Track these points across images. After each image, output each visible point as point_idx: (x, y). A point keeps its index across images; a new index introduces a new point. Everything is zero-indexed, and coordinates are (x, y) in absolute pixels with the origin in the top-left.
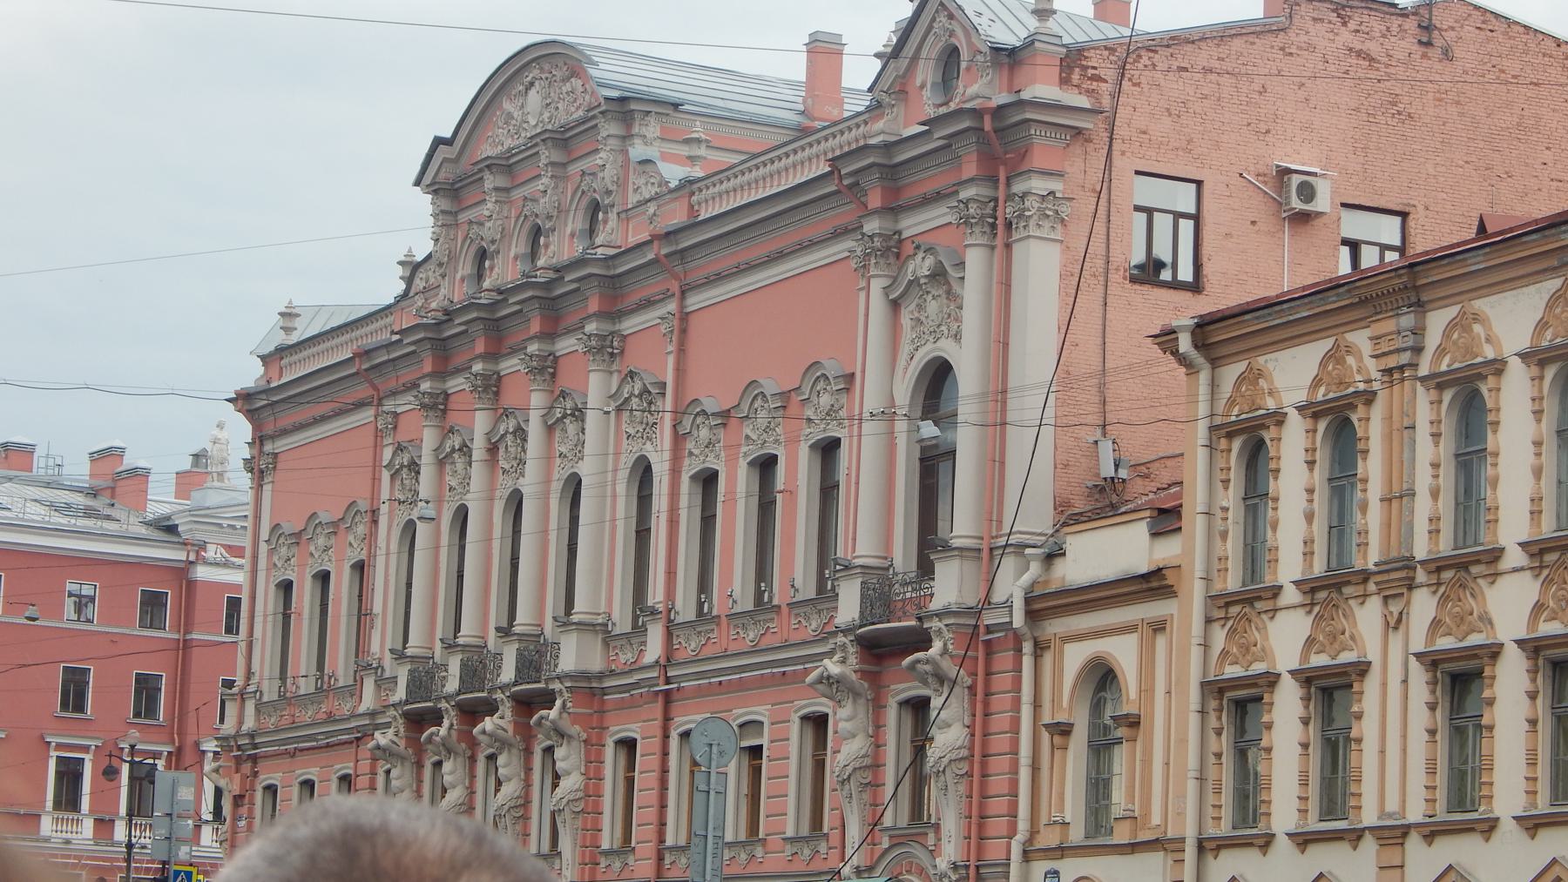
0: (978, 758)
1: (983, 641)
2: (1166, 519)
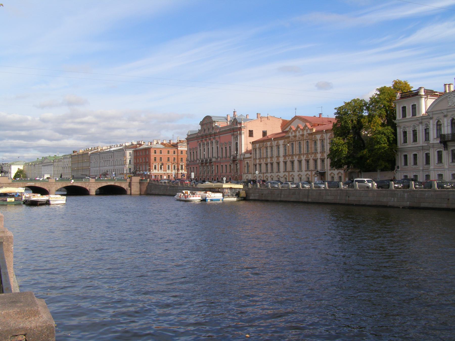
0: (241, 168)
1: (241, 161)
2: (251, 154)
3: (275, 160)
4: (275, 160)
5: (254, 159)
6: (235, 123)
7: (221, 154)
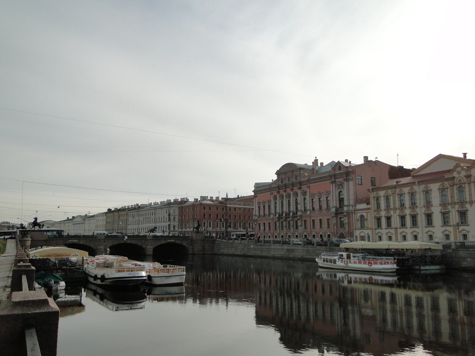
3: (421, 212)
4: (421, 212)
5: (375, 211)
6: (337, 168)
7: (263, 211)
